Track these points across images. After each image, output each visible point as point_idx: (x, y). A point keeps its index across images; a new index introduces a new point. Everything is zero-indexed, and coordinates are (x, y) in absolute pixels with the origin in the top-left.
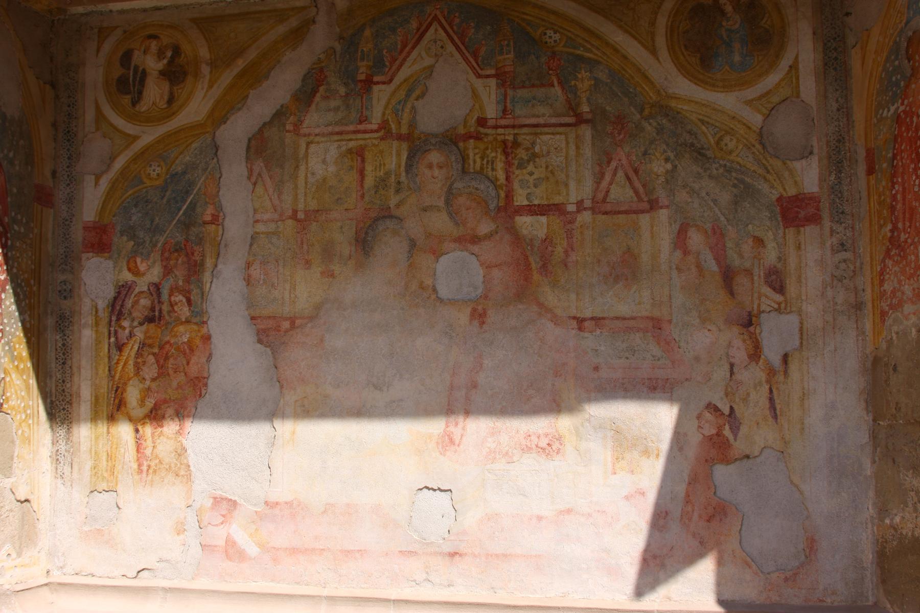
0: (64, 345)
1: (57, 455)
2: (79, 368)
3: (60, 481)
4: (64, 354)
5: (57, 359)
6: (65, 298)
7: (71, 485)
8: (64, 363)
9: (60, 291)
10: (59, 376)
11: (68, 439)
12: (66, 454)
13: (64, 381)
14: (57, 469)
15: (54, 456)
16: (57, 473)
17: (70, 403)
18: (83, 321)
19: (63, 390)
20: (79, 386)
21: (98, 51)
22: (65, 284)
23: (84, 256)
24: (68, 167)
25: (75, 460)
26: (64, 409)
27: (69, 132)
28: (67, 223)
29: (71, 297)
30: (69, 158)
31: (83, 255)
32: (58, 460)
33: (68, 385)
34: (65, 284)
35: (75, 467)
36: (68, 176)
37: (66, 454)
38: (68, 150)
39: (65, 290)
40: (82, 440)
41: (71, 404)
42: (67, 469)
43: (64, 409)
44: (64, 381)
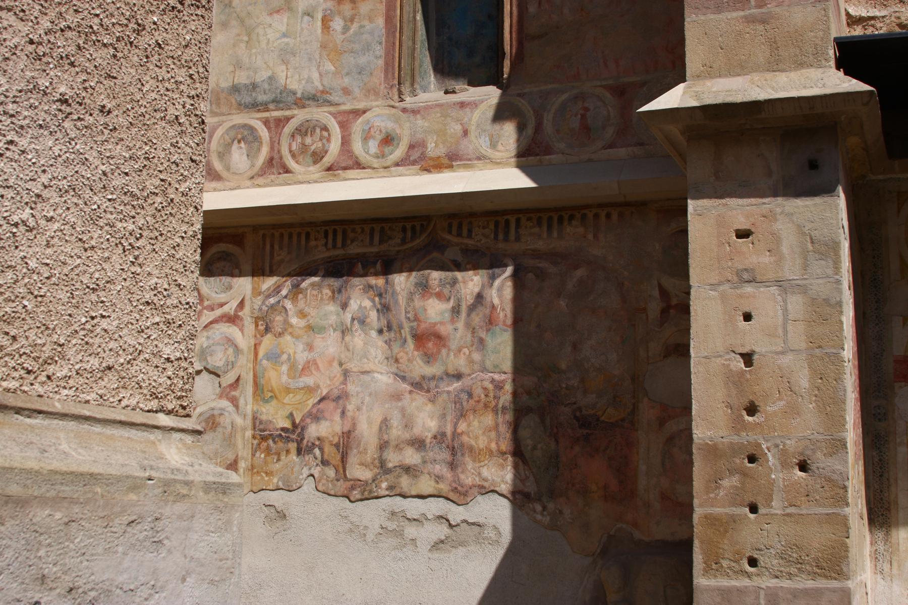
0: (880, 460)
1: (875, 554)
2: (896, 480)
3: (879, 577)
4: (881, 468)
5: (874, 472)
6: (880, 420)
7: (891, 580)
8: (881, 476)
9: (874, 415)
10: (877, 487)
11: (887, 540)
12: (885, 553)
13: (881, 491)
14: (876, 566)
15: (873, 555)
16: (876, 569)
17: (889, 510)
18: (898, 440)
19: (881, 499)
20: (896, 497)
21: (899, 211)
22: (879, 409)
23: (897, 385)
24: (876, 309)
25: (894, 558)
26: (882, 515)
27: (875, 279)
28: (878, 356)
29: (885, 419)
30: (876, 302)
31: (896, 384)
32: (877, 558)
33: (886, 495)
34: (879, 409)
35: (895, 564)
36: (877, 317)
37: (885, 553)
38: (876, 295)
39: (879, 414)
40: (901, 541)
41: (889, 511)
42: (886, 567)
43: (882, 515)
44: (881, 491)
